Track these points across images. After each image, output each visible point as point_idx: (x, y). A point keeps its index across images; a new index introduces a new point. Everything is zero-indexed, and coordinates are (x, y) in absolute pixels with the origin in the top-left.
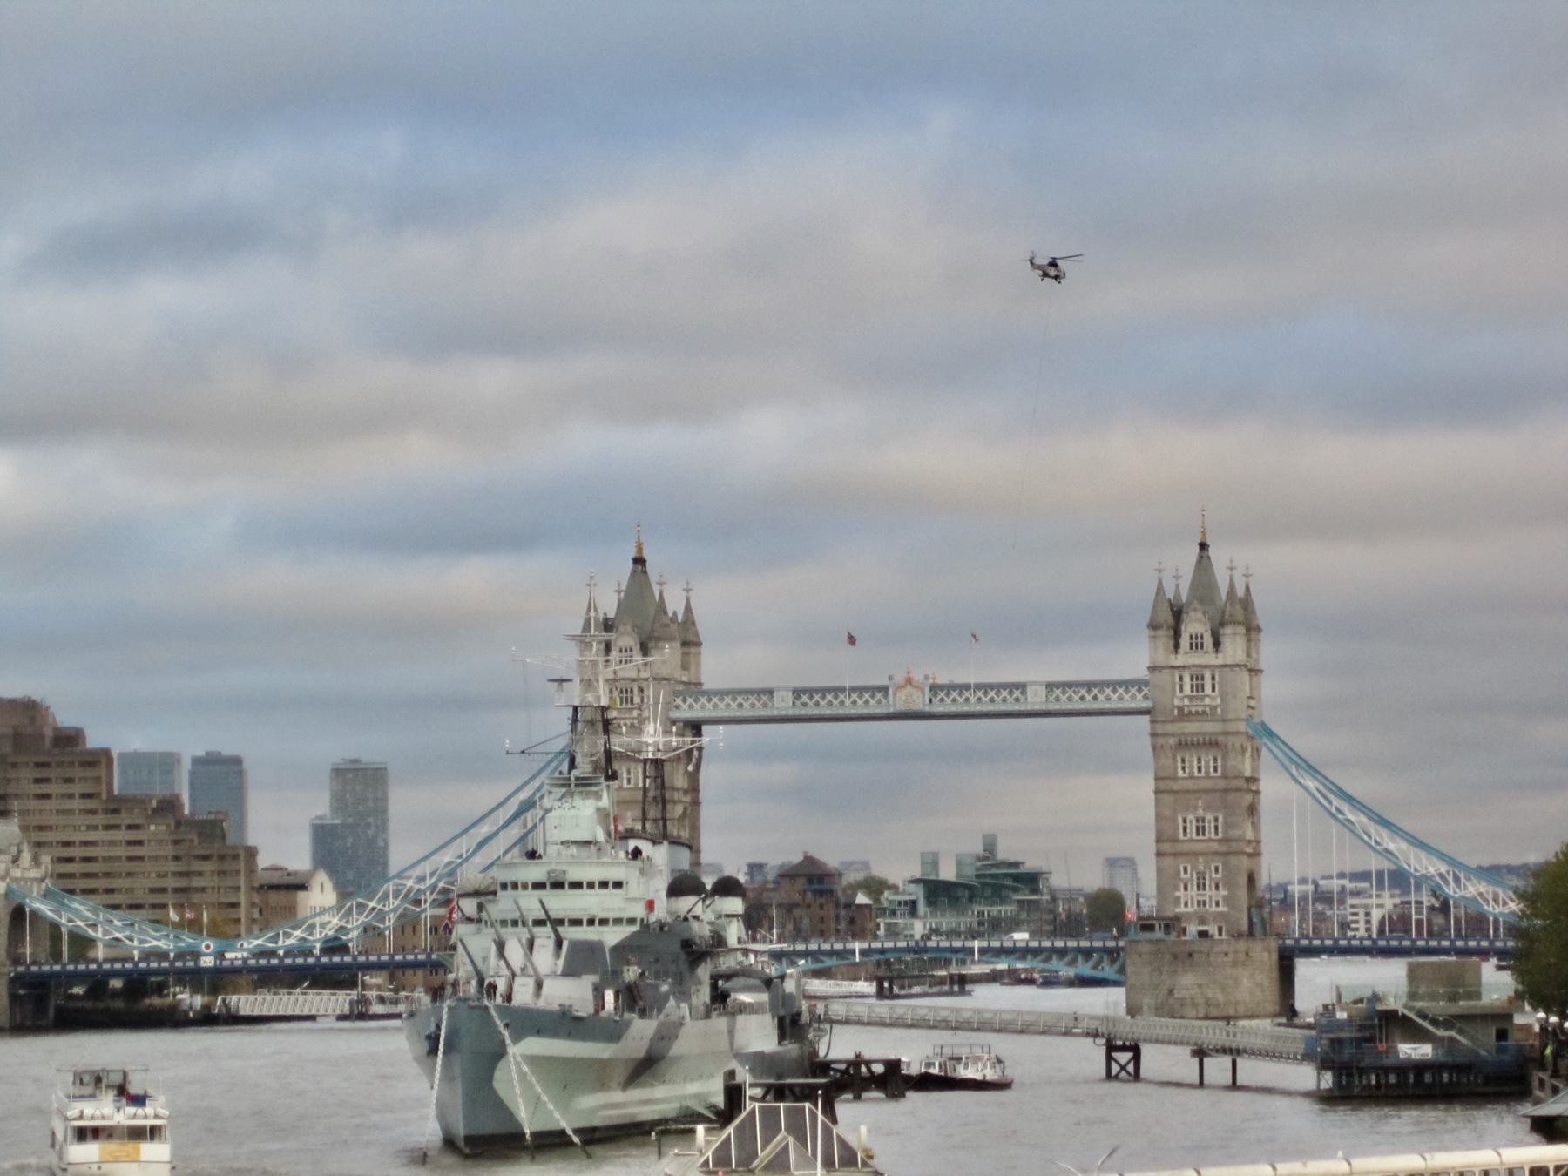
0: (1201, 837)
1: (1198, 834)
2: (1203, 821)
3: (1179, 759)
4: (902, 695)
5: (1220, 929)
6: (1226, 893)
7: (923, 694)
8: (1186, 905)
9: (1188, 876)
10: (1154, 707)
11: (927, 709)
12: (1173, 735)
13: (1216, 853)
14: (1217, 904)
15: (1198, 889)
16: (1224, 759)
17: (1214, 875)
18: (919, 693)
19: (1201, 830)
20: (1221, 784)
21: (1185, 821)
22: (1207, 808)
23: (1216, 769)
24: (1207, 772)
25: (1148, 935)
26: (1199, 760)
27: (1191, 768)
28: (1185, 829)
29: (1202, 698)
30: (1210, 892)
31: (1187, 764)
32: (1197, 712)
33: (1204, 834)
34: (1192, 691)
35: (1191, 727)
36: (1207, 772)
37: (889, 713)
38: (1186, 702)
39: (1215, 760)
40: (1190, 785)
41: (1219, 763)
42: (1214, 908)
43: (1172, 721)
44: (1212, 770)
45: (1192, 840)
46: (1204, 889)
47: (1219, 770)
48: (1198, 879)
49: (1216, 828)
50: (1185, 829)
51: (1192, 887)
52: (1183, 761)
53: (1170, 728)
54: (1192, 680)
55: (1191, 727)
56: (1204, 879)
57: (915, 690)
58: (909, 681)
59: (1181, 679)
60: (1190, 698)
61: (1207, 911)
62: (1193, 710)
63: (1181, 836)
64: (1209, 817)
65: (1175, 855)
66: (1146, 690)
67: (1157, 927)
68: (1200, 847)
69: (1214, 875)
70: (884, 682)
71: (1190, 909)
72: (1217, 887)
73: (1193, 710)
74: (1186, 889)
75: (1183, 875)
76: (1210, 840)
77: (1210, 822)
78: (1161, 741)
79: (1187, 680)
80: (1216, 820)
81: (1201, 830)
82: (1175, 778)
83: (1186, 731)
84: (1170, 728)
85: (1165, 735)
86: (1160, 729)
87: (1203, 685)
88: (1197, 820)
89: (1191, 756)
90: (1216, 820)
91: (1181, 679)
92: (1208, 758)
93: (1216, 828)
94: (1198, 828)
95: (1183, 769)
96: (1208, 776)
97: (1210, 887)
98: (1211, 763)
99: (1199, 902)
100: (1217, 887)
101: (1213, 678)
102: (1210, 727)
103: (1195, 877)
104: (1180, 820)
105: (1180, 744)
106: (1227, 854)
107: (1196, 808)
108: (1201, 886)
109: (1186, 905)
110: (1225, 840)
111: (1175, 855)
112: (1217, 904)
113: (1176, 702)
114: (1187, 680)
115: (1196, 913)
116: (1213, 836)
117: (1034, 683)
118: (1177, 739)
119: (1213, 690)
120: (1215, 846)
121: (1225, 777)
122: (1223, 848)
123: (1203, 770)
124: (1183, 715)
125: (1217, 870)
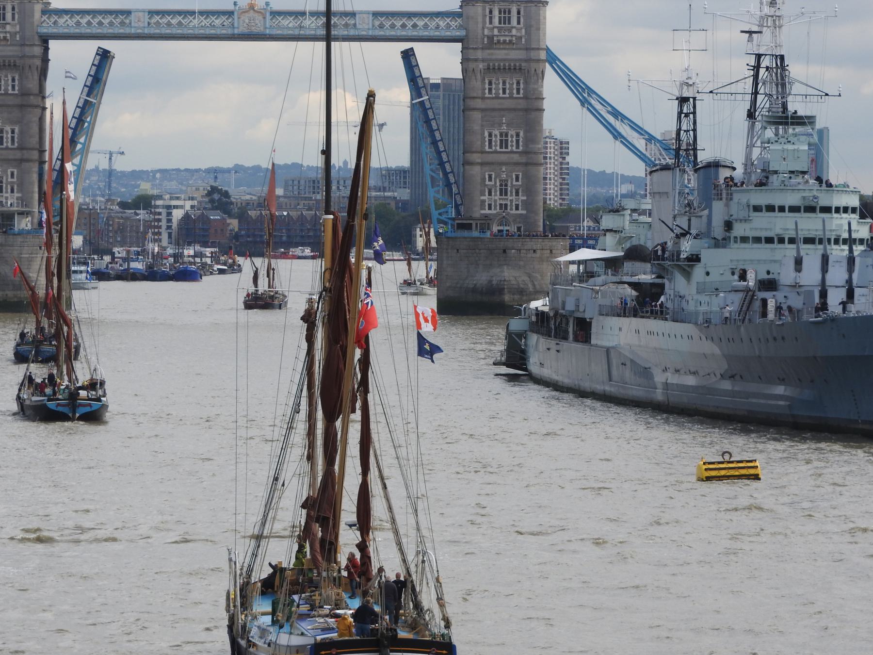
0: (504, 150)
1: (501, 147)
2: (507, 135)
3: (487, 82)
4: (245, 18)
5: (519, 229)
6: (525, 198)
7: (264, 18)
8: (490, 208)
9: (520, 183)
10: (466, 36)
11: (268, 32)
12: (483, 61)
13: (517, 164)
14: (517, 209)
15: (501, 195)
16: (526, 83)
17: (515, 183)
18: (261, 18)
19: (504, 143)
20: (522, 104)
21: (490, 135)
22: (508, 125)
23: (518, 93)
24: (511, 93)
25: (466, 233)
26: (504, 83)
27: (497, 89)
28: (490, 141)
29: (510, 30)
30: (510, 197)
31: (494, 86)
32: (505, 41)
33: (506, 147)
34: (500, 23)
35: (500, 54)
36: (511, 93)
37: (234, 35)
38: (496, 32)
39: (518, 83)
40: (496, 104)
41: (522, 86)
42: (514, 212)
43: (482, 49)
44: (515, 91)
45: (496, 152)
46: (506, 194)
47: (522, 91)
48: (501, 185)
49: (518, 141)
50: (490, 141)
51: (496, 192)
52: (490, 83)
53: (479, 54)
54: (500, 13)
55: (500, 54)
56: (506, 185)
57: (256, 15)
58: (252, 7)
59: (491, 12)
60: (500, 29)
61: (508, 214)
62: (502, 39)
63: (487, 149)
64: (512, 132)
65: (482, 164)
66: (459, 20)
67: (474, 226)
68: (504, 158)
69: (515, 183)
70: (230, 7)
71: (493, 212)
72: (517, 194)
73: (502, 39)
74: (490, 194)
75: (487, 182)
76: (512, 152)
77: (512, 136)
78: (472, 65)
79: (496, 13)
80: (518, 135)
81: (504, 143)
82: (483, 98)
83: (494, 57)
84: (479, 54)
85: (476, 60)
86: (472, 55)
87: (509, 18)
88: (501, 135)
89: (511, 78)
90: (518, 135)
91: (491, 12)
92: (511, 81)
93: (518, 141)
94: (501, 141)
95: (490, 90)
96: (511, 97)
97: (511, 193)
98: (515, 86)
99: (501, 205)
100: (517, 194)
101: (519, 13)
102: (515, 55)
103: (498, 184)
104: (486, 134)
105: (489, 68)
106: (526, 164)
107: (500, 124)
108: (504, 192)
109: (490, 208)
110: (526, 153)
111: (482, 164)
112: (517, 209)
113: (486, 32)
114: (496, 13)
115: (498, 214)
116: (514, 148)
117: (361, 13)
118: (486, 64)
119: (519, 23)
120: (516, 158)
121: (526, 97)
122: (523, 160)
123: (507, 91)
124: (492, 43)
125: (517, 180)
